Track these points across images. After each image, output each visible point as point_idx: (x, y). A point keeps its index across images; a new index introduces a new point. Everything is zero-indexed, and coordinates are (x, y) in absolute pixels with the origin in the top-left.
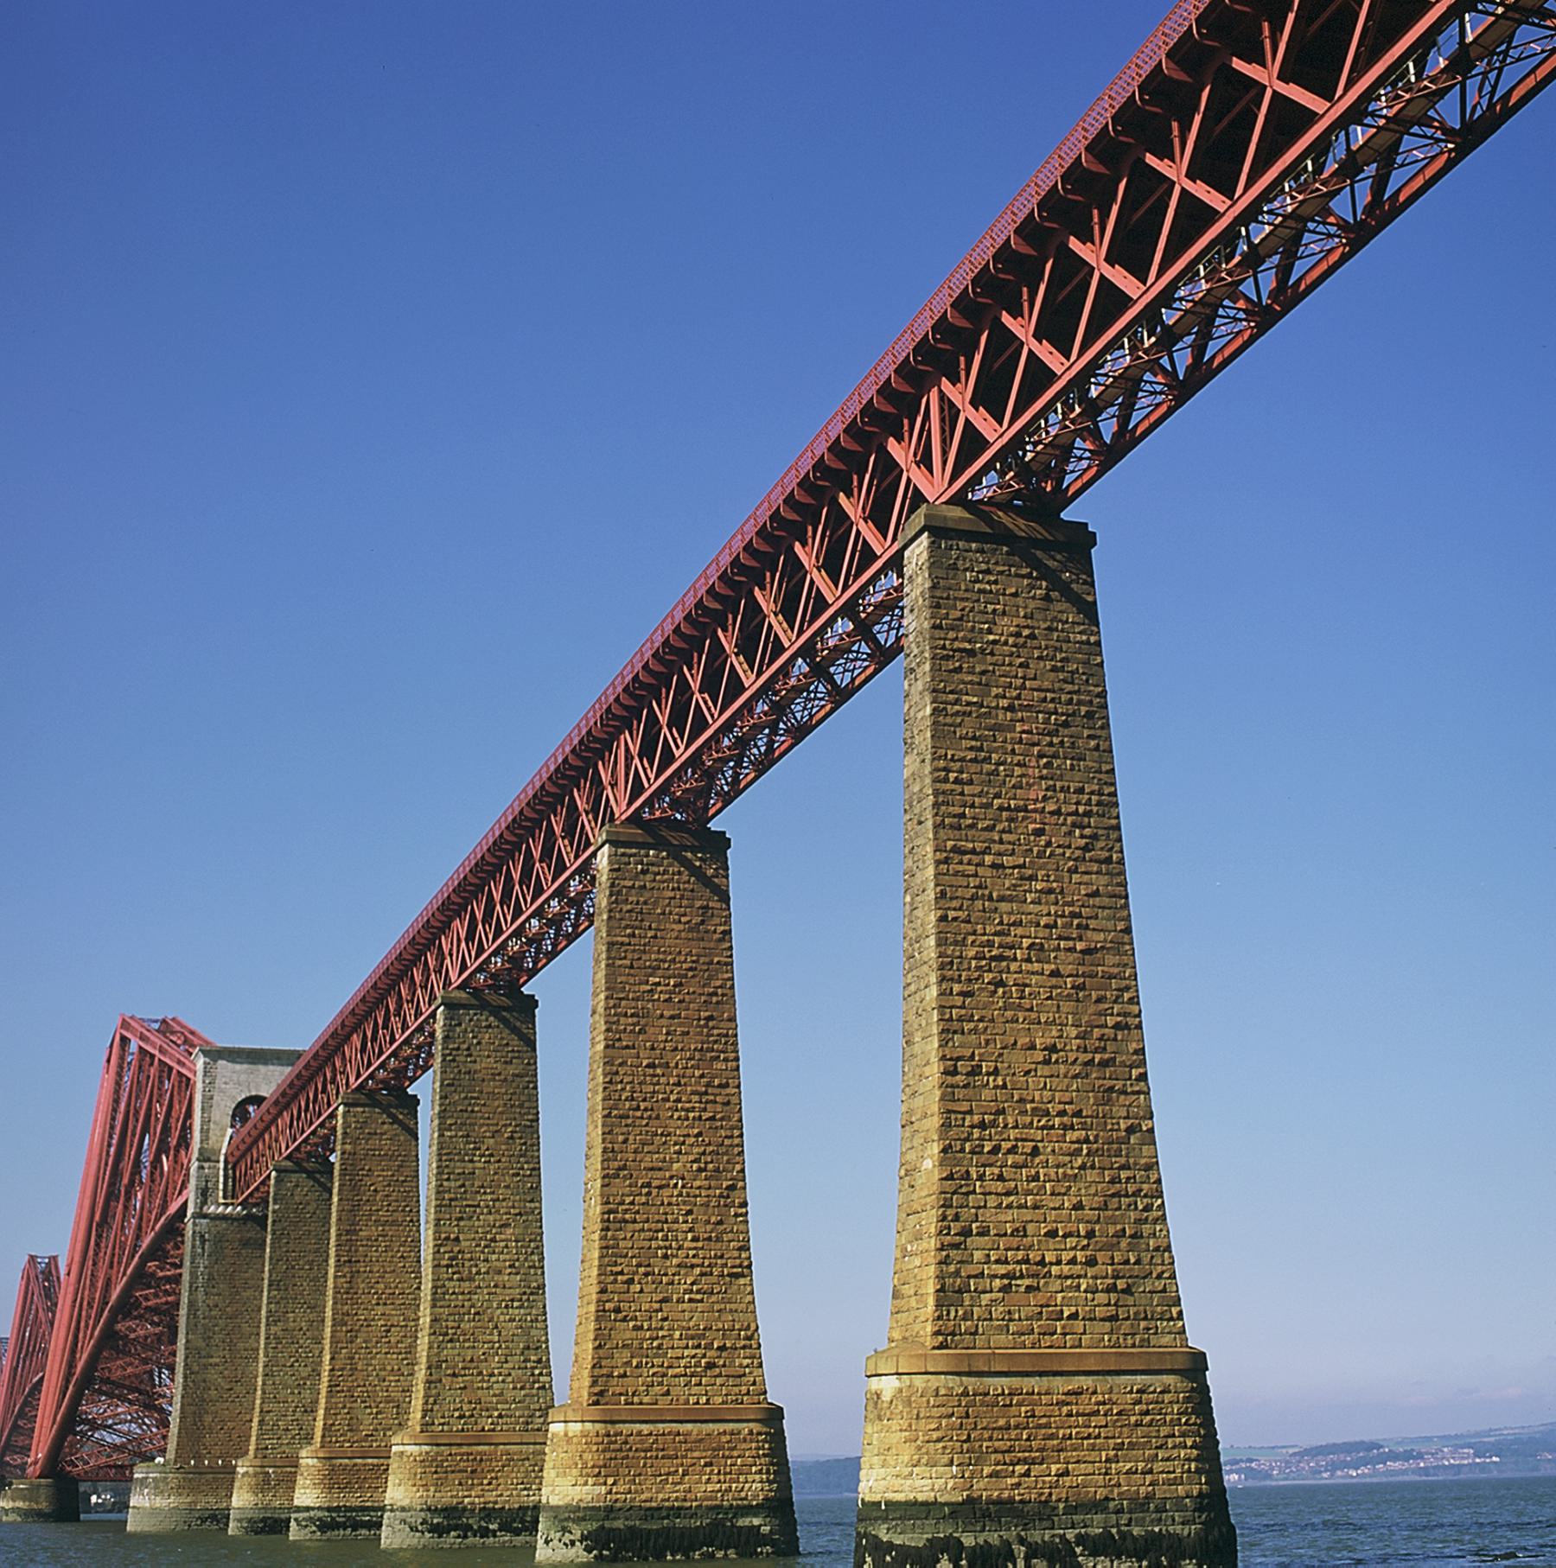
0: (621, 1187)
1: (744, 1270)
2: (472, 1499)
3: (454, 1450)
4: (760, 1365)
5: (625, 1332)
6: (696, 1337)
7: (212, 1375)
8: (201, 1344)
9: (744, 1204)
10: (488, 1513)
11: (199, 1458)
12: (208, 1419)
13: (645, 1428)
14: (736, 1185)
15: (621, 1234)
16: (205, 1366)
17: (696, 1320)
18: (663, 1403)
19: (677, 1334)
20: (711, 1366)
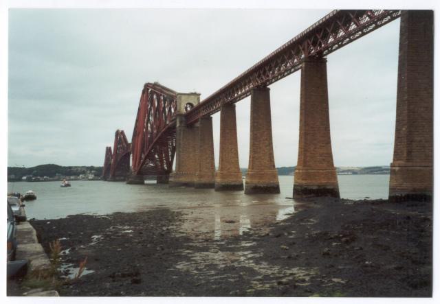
5: (308, 154)
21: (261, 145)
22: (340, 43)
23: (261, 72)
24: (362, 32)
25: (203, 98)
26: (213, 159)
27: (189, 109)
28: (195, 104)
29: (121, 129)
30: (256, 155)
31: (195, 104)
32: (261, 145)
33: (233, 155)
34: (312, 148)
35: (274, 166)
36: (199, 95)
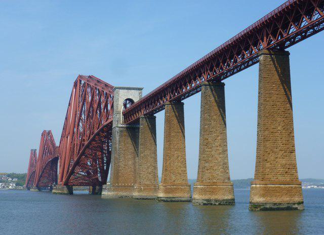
0: (267, 132)
1: (293, 151)
2: (213, 197)
3: (209, 187)
4: (297, 172)
5: (268, 165)
6: (283, 166)
7: (120, 164)
8: (118, 157)
9: (293, 137)
10: (216, 201)
11: (118, 183)
12: (120, 174)
13: (273, 186)
14: (292, 132)
15: (268, 143)
16: (119, 162)
17: (284, 162)
18: (277, 180)
19: (279, 165)
20: (286, 172)
21: (213, 153)
22: (303, 35)
23: (174, 88)
24: (302, 36)
25: (146, 93)
26: (156, 168)
27: (128, 106)
28: (136, 100)
29: (47, 129)
30: (207, 165)
31: (136, 100)
32: (213, 153)
33: (180, 164)
34: (272, 158)
35: (229, 179)
36: (140, 89)
